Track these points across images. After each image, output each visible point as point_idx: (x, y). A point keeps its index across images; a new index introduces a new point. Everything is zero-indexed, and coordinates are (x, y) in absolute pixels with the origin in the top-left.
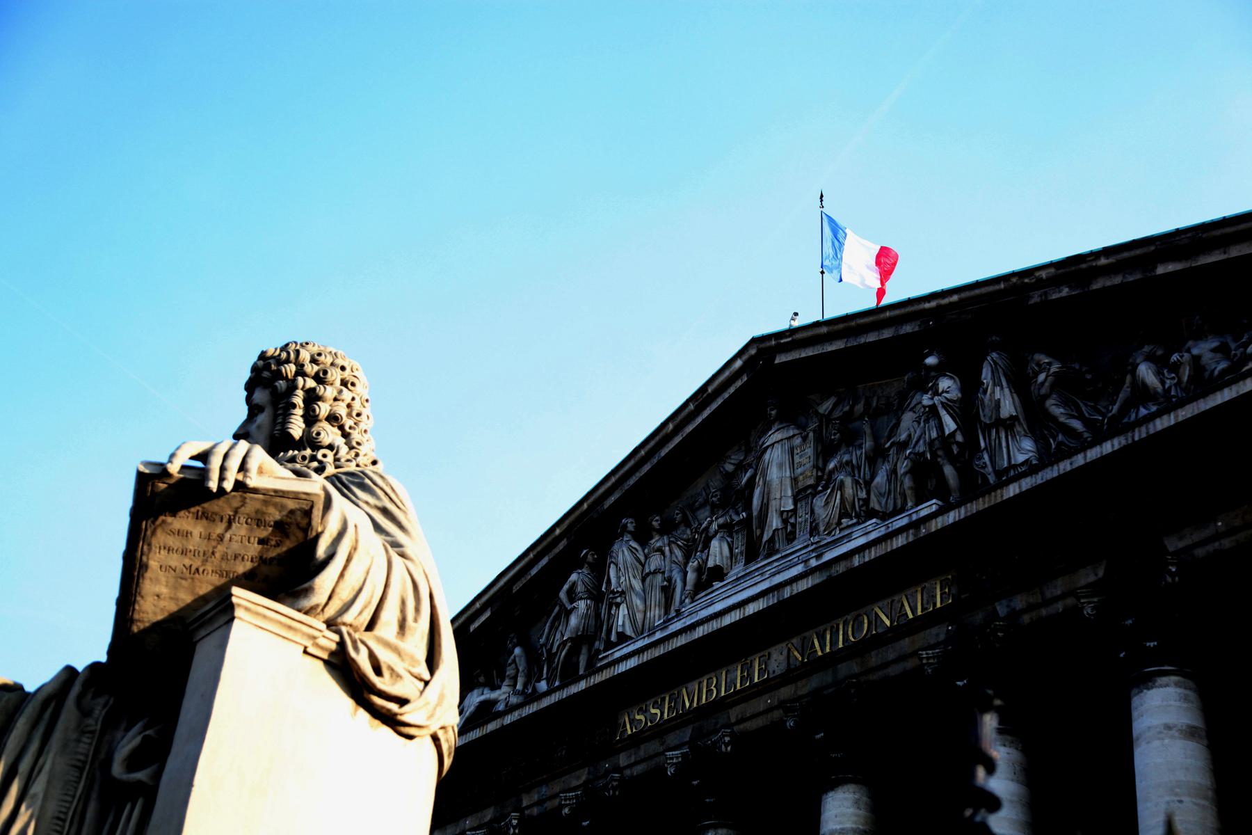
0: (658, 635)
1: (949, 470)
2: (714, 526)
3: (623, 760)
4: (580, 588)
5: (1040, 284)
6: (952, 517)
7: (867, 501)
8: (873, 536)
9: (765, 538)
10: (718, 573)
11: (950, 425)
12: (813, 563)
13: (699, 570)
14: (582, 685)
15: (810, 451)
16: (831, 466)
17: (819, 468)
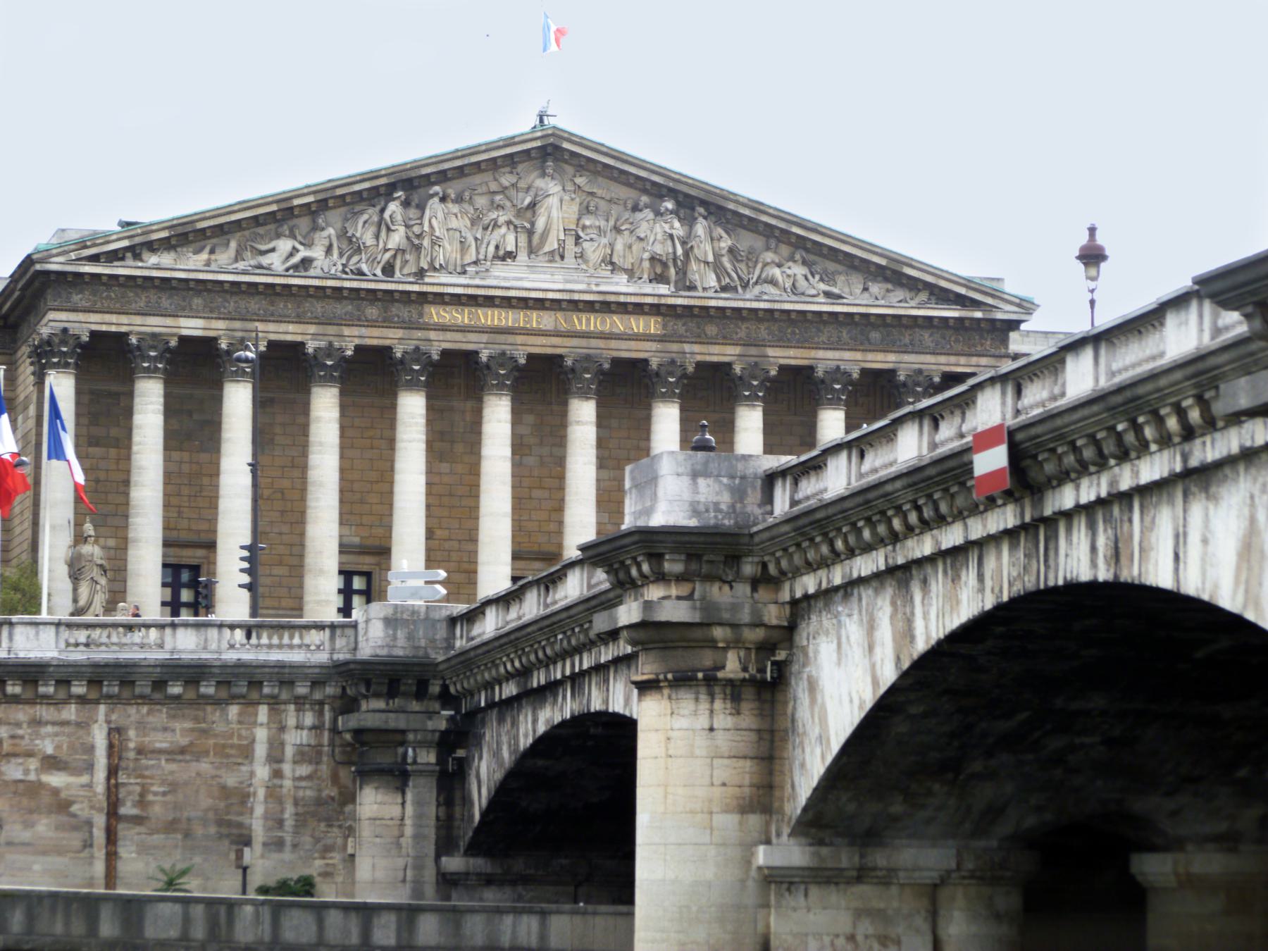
0: (477, 282)
1: (672, 271)
2: (502, 220)
3: (432, 335)
4: (399, 217)
5: (737, 202)
6: (679, 301)
7: (611, 255)
8: (631, 290)
9: (547, 249)
10: (510, 255)
11: (680, 251)
12: (594, 288)
13: (497, 247)
14: (416, 288)
15: (575, 208)
16: (587, 222)
17: (579, 220)
